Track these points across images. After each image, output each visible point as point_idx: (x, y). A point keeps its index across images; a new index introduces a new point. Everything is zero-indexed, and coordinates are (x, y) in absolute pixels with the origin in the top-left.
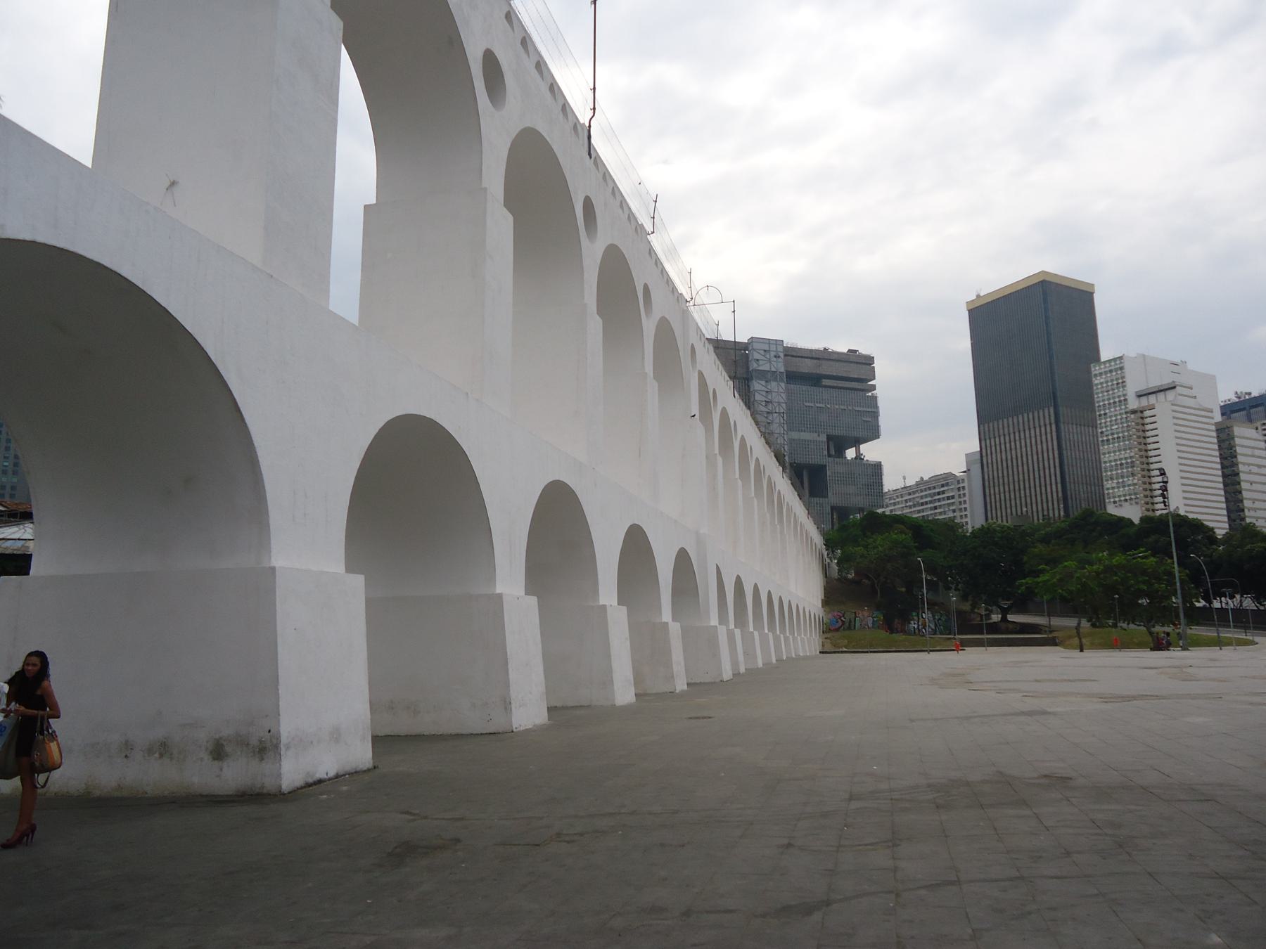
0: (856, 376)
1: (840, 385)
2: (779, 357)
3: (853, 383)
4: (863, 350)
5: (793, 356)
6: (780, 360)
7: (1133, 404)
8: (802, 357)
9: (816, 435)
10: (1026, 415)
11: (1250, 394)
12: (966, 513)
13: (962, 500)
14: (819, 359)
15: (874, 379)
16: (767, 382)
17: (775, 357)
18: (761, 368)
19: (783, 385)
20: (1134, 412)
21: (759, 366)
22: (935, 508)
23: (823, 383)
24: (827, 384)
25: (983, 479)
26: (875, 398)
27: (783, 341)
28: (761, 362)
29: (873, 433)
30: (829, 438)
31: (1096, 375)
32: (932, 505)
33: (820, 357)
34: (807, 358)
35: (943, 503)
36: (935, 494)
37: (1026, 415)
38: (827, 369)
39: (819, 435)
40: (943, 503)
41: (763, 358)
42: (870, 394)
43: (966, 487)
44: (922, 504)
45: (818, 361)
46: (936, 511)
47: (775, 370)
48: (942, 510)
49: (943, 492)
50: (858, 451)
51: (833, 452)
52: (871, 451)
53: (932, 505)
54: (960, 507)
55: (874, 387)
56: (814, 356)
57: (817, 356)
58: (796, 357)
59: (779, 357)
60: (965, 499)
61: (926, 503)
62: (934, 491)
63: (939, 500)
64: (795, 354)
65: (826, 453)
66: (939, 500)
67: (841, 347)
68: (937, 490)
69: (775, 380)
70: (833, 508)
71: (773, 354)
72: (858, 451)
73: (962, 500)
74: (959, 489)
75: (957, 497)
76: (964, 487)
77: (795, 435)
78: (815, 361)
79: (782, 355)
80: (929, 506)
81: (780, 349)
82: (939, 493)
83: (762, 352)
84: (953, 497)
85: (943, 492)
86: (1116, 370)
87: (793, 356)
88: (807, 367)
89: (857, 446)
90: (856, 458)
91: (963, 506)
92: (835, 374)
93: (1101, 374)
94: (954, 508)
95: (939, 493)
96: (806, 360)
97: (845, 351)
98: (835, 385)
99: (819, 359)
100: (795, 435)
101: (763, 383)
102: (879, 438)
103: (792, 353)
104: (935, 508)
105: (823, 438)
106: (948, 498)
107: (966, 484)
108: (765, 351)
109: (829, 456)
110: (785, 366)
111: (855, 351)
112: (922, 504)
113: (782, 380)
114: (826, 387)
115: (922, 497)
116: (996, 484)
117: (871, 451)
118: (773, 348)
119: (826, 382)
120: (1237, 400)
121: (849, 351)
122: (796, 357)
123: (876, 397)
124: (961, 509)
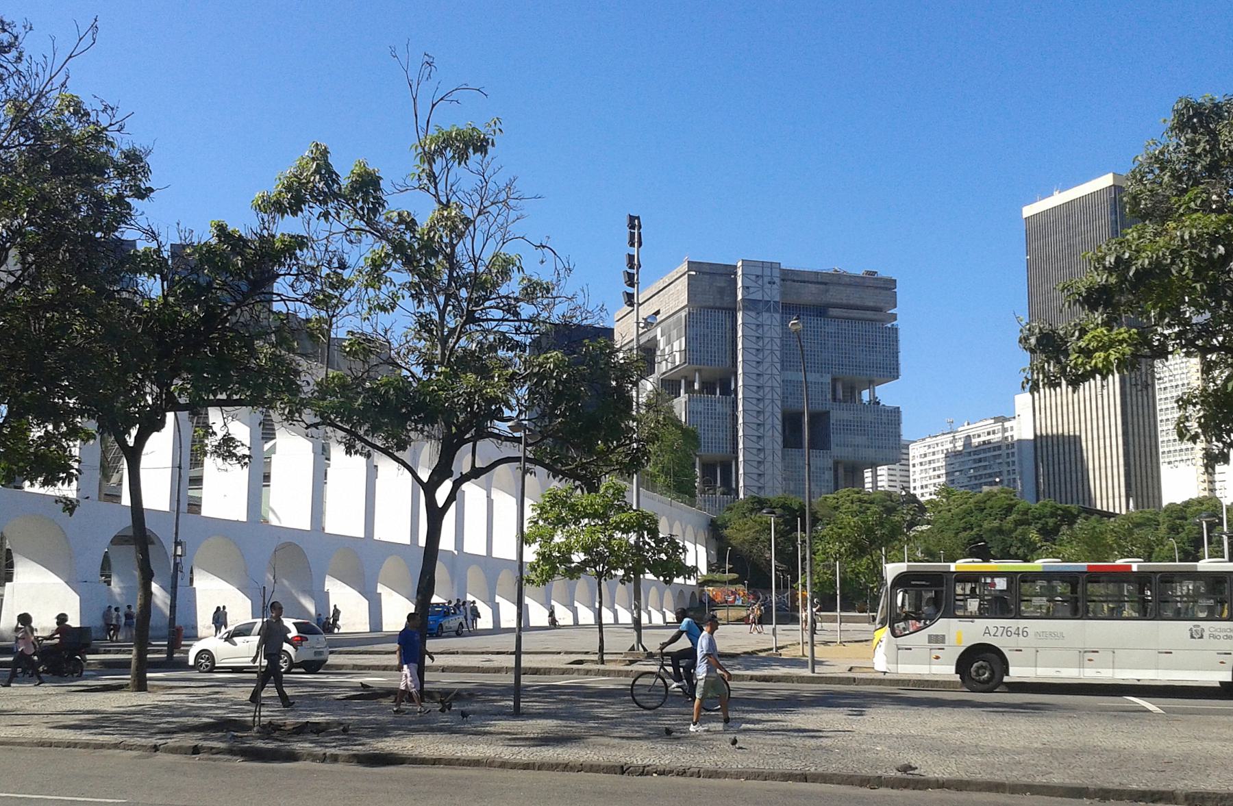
0: (871, 304)
2: (774, 283)
4: (883, 273)
5: (794, 281)
6: (775, 286)
8: (804, 282)
9: (818, 375)
13: (1010, 451)
14: (826, 284)
17: (769, 283)
18: (750, 297)
19: (778, 316)
21: (749, 294)
22: (980, 460)
23: (831, 313)
24: (835, 314)
26: (895, 330)
27: (780, 264)
28: (752, 290)
29: (892, 372)
30: (834, 380)
32: (976, 457)
34: (811, 283)
35: (988, 454)
38: (835, 295)
39: (822, 376)
40: (988, 454)
41: (754, 284)
42: (889, 325)
45: (824, 286)
46: (980, 464)
47: (769, 299)
48: (987, 463)
51: (840, 394)
52: (887, 394)
53: (976, 457)
55: (894, 317)
56: (820, 280)
57: (823, 281)
58: (798, 281)
59: (774, 283)
60: (1013, 450)
64: (795, 278)
65: (829, 396)
67: (857, 269)
69: (768, 310)
70: (836, 464)
71: (766, 279)
72: (873, 394)
73: (1010, 451)
78: (822, 287)
79: (777, 280)
81: (776, 273)
83: (753, 278)
87: (794, 281)
88: (809, 295)
89: (871, 386)
92: (845, 302)
94: (1000, 461)
96: (810, 285)
97: (858, 270)
98: (845, 315)
99: (826, 284)
102: (898, 378)
103: (790, 277)
105: (827, 379)
108: (757, 276)
109: (834, 399)
110: (783, 294)
113: (776, 311)
117: (887, 394)
118: (767, 272)
119: (833, 312)
121: (869, 273)
122: (798, 281)
124: (1008, 463)
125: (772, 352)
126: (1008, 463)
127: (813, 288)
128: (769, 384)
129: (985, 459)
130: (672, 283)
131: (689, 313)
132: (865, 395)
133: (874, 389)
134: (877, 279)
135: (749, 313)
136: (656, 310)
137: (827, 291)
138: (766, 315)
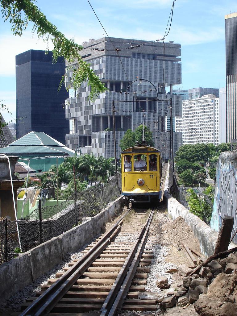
0: (172, 54)
3: (171, 58)
4: (176, 42)
14: (156, 46)
15: (181, 55)
23: (157, 58)
24: (159, 58)
25: (227, 101)
26: (180, 65)
33: (157, 45)
38: (160, 51)
76: (217, 104)
99: (156, 46)
111: (172, 42)
114: (158, 60)
116: (232, 104)
119: (158, 57)
123: (181, 64)
127: (151, 48)
130: (97, 44)
131: (106, 58)
132: (168, 89)
133: (172, 86)
134: (174, 44)
136: (89, 54)
137: (157, 49)
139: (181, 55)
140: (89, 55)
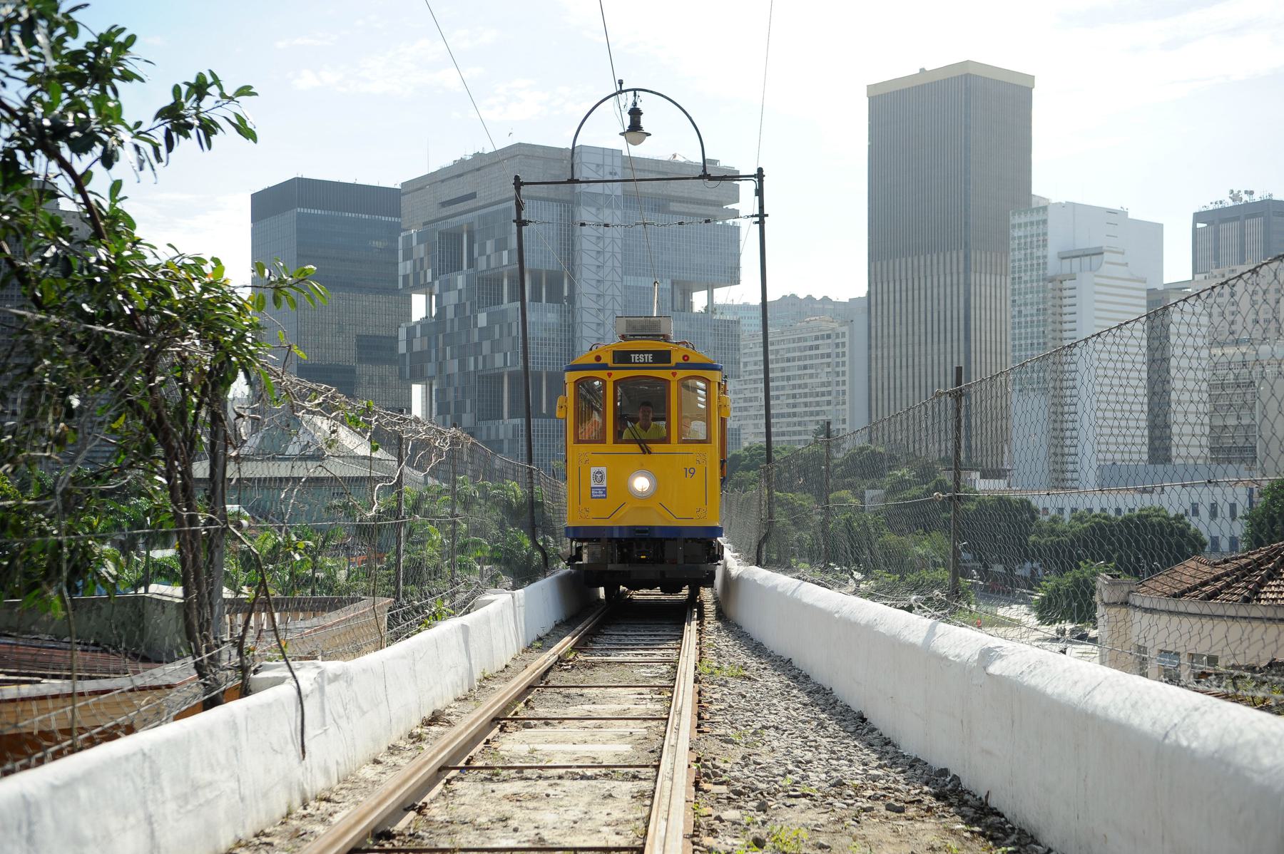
0: (713, 198)
1: (693, 211)
7: (1053, 267)
10: (929, 256)
11: (1251, 193)
12: (843, 369)
13: (840, 360)
15: (737, 201)
16: (598, 209)
20: (1052, 280)
22: (805, 367)
23: (671, 209)
24: (676, 209)
31: (1014, 226)
32: (801, 363)
36: (805, 349)
37: (929, 256)
43: (847, 345)
44: (788, 360)
47: (610, 193)
48: (813, 371)
49: (817, 347)
50: (710, 297)
53: (801, 363)
54: (837, 369)
60: (844, 359)
61: (794, 359)
62: (805, 344)
63: (811, 357)
65: (669, 305)
66: (811, 357)
68: (809, 343)
69: (609, 206)
72: (710, 297)
73: (840, 360)
74: (837, 345)
75: (834, 355)
76: (844, 344)
77: (630, 281)
80: (797, 363)
81: (618, 162)
82: (811, 348)
83: (593, 167)
84: (829, 356)
85: (817, 347)
86: (1038, 223)
90: (707, 308)
91: (840, 369)
92: (686, 195)
93: (1020, 225)
95: (811, 348)
98: (687, 210)
100: (630, 281)
101: (593, 210)
104: (805, 367)
106: (822, 356)
107: (846, 340)
108: (598, 165)
112: (788, 360)
113: (618, 207)
115: (789, 350)
118: (608, 161)
119: (674, 206)
120: (1231, 203)
125: (613, 255)
126: (838, 374)
128: (610, 292)
129: (812, 366)
132: (699, 300)
135: (589, 209)
136: (469, 191)
138: (607, 212)
139: (737, 201)
140: (472, 196)
